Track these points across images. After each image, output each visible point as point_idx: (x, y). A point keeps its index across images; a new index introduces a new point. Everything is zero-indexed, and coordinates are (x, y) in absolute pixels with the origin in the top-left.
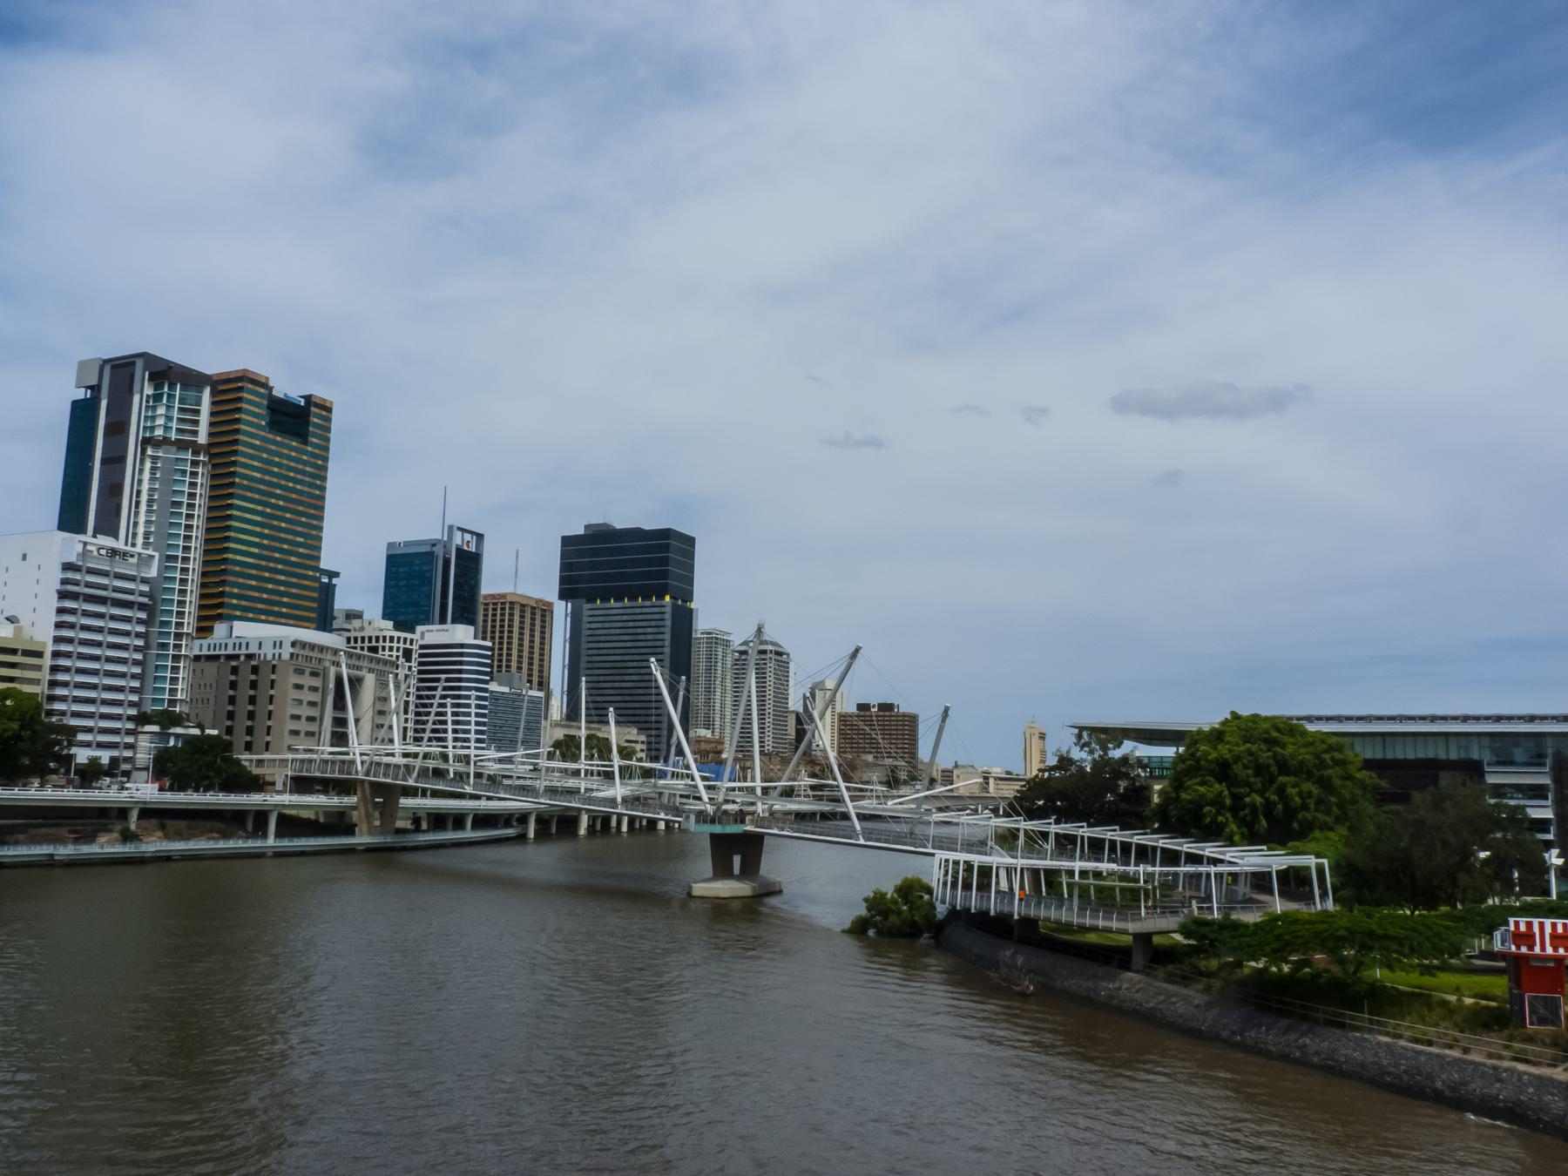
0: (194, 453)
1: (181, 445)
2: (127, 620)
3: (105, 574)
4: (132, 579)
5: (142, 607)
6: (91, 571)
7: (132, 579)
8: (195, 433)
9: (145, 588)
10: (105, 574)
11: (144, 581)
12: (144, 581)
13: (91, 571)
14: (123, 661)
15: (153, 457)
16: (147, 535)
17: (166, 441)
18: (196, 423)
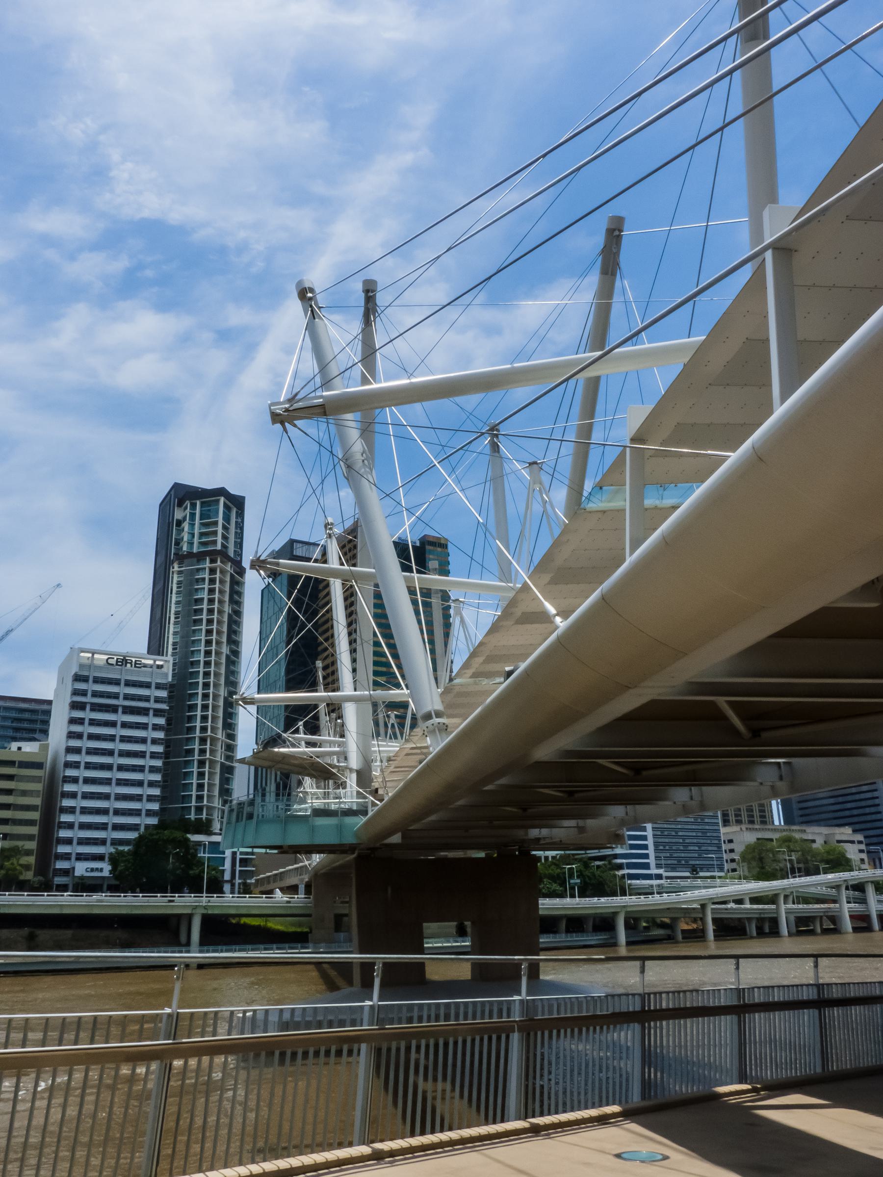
0: (213, 561)
1: (200, 557)
2: (144, 727)
3: (117, 682)
4: (147, 685)
5: (158, 713)
6: (97, 680)
7: (147, 685)
8: (215, 542)
9: (164, 694)
10: (117, 682)
11: (159, 687)
12: (159, 687)
13: (97, 680)
14: (141, 769)
15: (179, 573)
16: (174, 644)
17: (190, 555)
18: (215, 533)
